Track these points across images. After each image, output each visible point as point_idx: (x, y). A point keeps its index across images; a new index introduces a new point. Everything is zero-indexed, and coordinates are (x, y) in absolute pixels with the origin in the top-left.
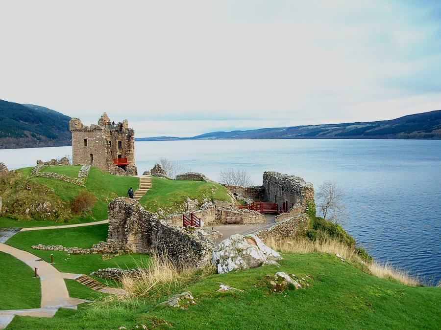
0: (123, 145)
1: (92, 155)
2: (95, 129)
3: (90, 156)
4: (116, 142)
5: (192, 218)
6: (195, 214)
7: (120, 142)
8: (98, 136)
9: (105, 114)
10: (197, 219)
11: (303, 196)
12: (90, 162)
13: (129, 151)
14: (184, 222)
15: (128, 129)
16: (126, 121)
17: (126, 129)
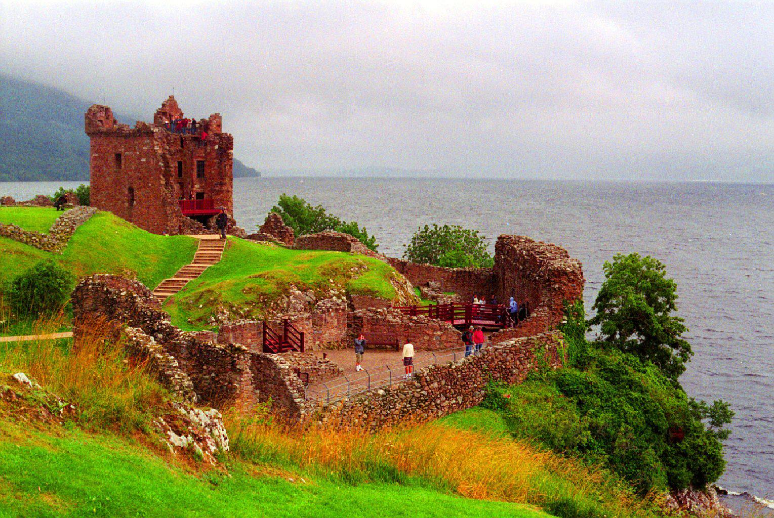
0: (207, 170)
1: (131, 190)
2: (142, 131)
3: (126, 192)
4: (193, 165)
5: (286, 330)
6: (295, 321)
7: (201, 165)
8: (145, 148)
9: (171, 98)
10: (297, 335)
11: (554, 289)
12: (127, 204)
13: (221, 184)
14: (265, 339)
15: (220, 135)
16: (217, 117)
17: (216, 135)
